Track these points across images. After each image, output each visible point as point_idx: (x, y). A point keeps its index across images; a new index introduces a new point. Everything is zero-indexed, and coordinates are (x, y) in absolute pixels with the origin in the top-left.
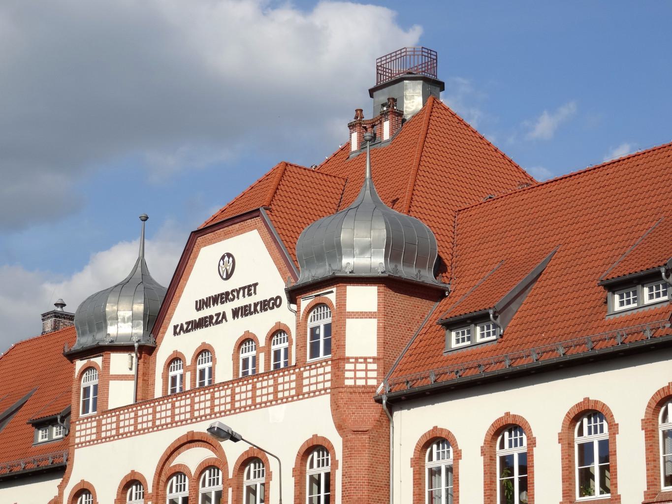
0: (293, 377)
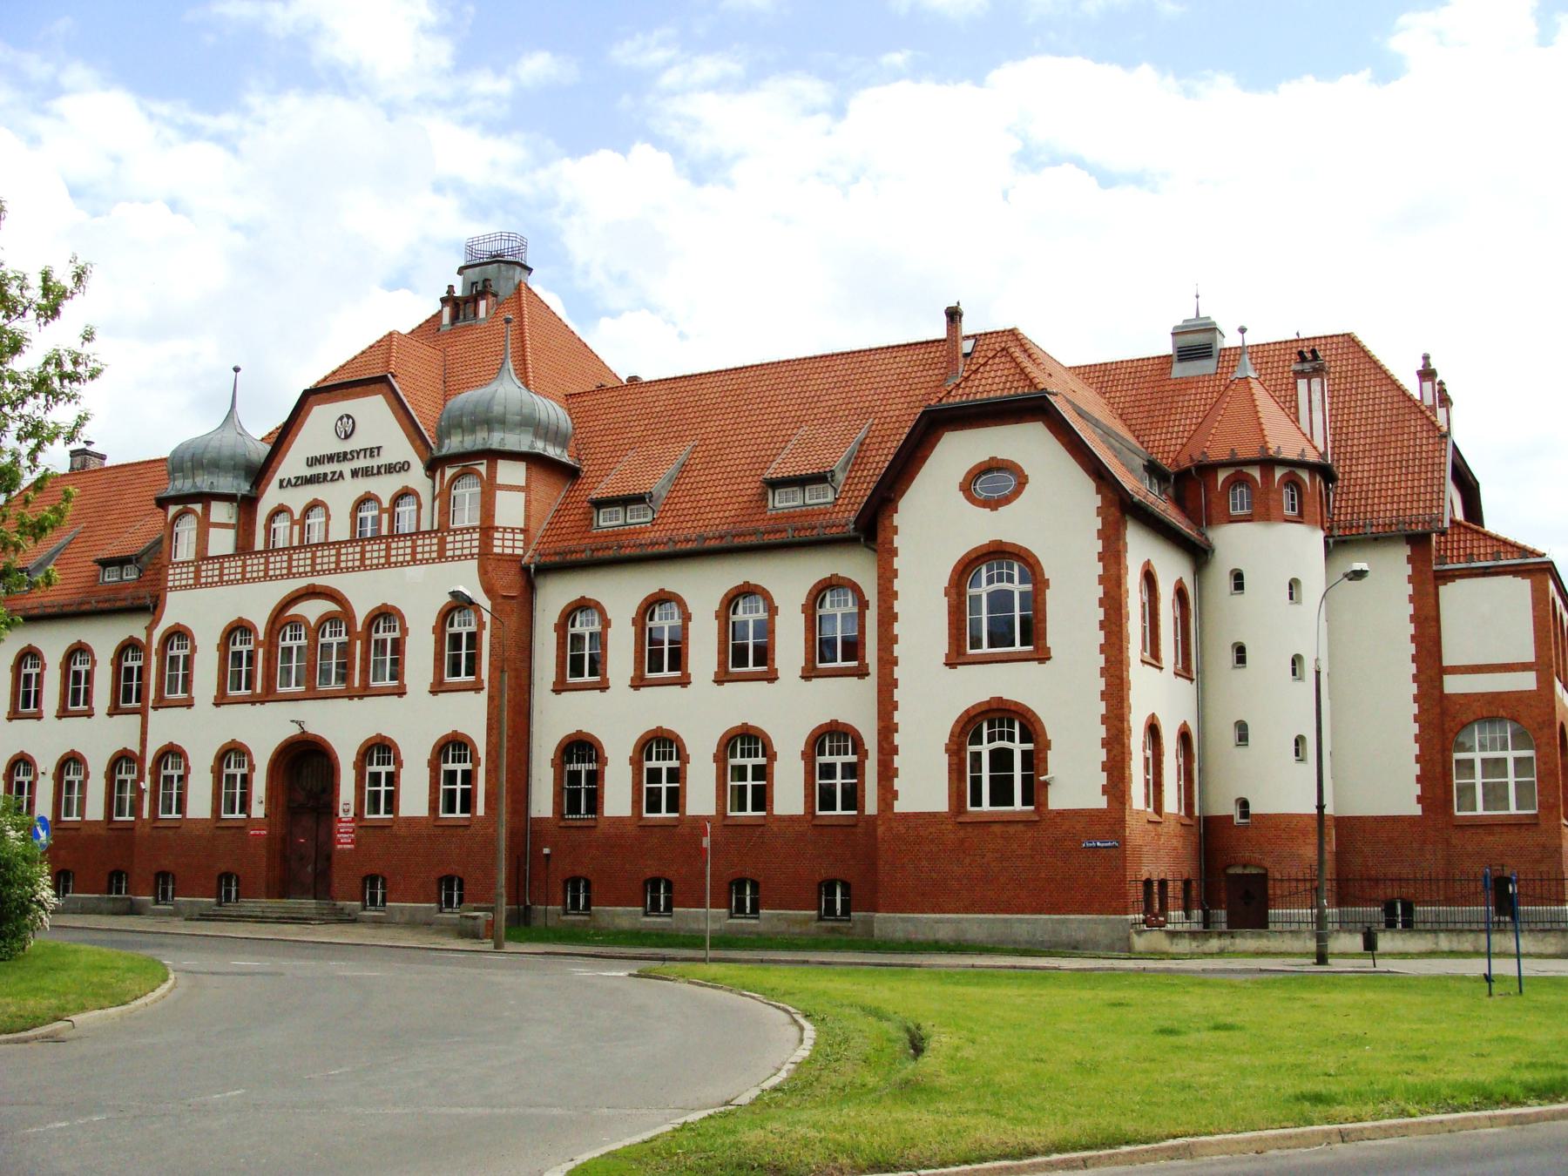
0: (435, 541)
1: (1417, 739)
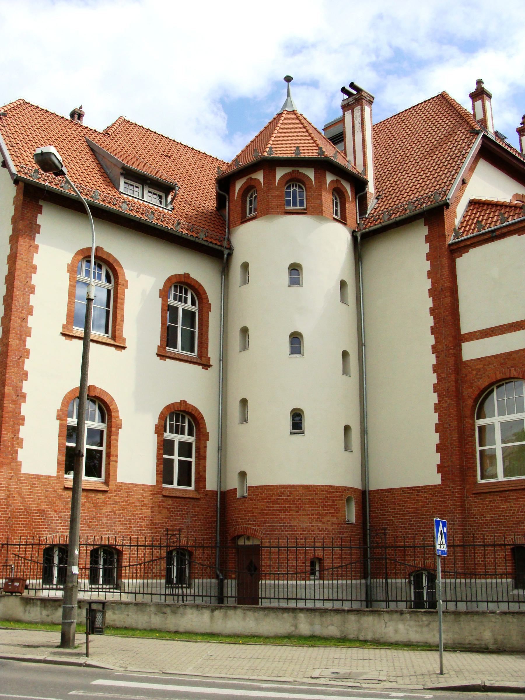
1: (438, 408)
